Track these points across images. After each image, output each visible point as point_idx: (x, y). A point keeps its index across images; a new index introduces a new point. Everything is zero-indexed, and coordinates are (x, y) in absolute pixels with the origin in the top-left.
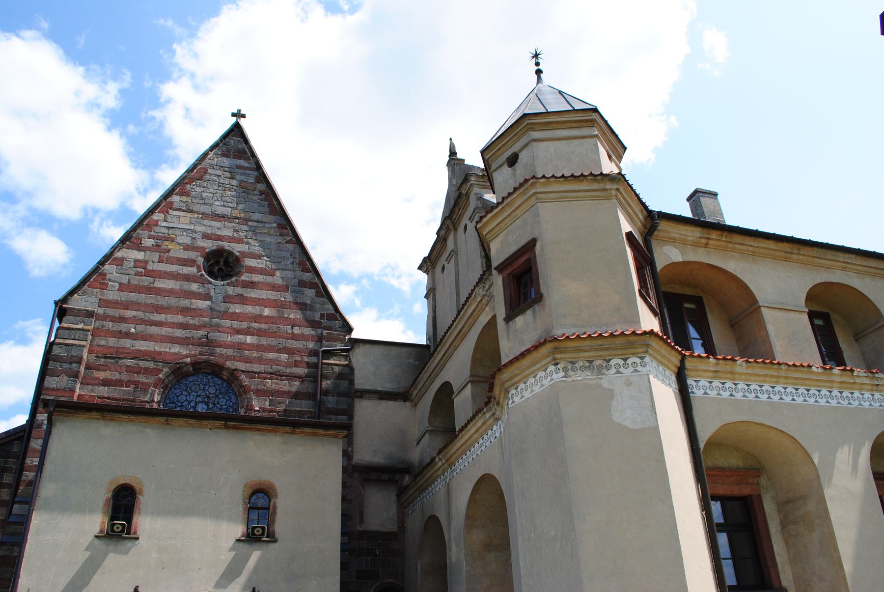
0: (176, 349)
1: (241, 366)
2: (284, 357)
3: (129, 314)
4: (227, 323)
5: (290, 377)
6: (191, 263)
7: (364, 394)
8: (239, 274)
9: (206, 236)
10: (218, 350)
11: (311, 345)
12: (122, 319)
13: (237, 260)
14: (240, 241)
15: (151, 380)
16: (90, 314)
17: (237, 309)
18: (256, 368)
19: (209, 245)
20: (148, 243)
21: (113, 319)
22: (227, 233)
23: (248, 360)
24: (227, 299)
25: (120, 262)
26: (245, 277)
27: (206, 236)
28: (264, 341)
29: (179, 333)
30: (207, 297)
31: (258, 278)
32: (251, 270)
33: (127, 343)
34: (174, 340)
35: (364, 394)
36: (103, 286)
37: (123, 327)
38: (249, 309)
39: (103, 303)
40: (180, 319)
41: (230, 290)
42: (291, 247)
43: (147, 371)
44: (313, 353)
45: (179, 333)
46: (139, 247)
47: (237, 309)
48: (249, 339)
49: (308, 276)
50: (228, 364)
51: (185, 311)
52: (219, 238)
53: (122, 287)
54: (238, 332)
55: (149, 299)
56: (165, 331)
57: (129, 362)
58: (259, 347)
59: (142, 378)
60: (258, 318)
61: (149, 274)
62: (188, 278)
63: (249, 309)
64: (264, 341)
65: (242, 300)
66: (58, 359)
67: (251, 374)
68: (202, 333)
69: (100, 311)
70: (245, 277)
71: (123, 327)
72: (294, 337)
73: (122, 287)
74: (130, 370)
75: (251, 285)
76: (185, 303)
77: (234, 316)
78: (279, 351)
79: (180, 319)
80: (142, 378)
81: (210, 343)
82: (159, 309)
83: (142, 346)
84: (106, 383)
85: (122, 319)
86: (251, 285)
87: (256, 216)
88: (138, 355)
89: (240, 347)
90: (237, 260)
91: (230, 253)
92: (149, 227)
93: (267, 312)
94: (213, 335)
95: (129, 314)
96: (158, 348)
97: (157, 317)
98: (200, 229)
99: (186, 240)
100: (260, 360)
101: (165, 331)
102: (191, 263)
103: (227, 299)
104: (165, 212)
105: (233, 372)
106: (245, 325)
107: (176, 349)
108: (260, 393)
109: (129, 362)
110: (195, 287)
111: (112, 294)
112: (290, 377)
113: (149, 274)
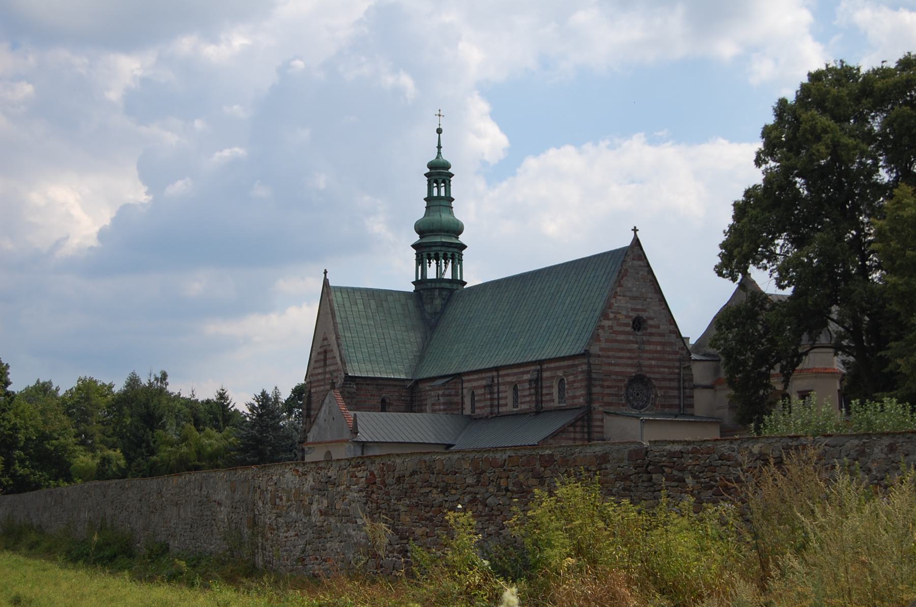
0: (629, 370)
1: (653, 376)
2: (666, 370)
3: (611, 353)
4: (645, 355)
5: (671, 380)
6: (627, 325)
7: (695, 387)
8: (646, 329)
9: (633, 310)
10: (644, 369)
11: (677, 364)
12: (609, 357)
13: (645, 321)
14: (644, 310)
15: (623, 384)
16: (599, 356)
17: (648, 347)
18: (658, 376)
19: (633, 314)
20: (612, 316)
21: (606, 357)
22: (639, 307)
23: (654, 373)
24: (643, 343)
25: (603, 327)
26: (649, 331)
27: (633, 310)
28: (660, 363)
29: (629, 362)
30: (637, 343)
31: (654, 330)
32: (651, 326)
33: (612, 368)
34: (628, 365)
35: (695, 387)
36: (600, 341)
37: (609, 360)
38: (652, 347)
39: (601, 349)
40: (628, 354)
41: (645, 338)
42: (664, 311)
43: (620, 381)
44: (679, 368)
45: (629, 362)
46: (609, 319)
47: (648, 347)
48: (653, 362)
49: (672, 327)
50: (648, 375)
51: (630, 350)
52: (637, 310)
53: (607, 340)
54: (650, 359)
55: (616, 345)
56: (624, 361)
57: (613, 377)
58: (658, 367)
59: (619, 384)
60: (656, 352)
61: (614, 332)
62: (628, 333)
63: (652, 347)
64: (660, 363)
65: (650, 343)
66: (595, 379)
67: (656, 379)
68: (635, 361)
69: (600, 353)
70: (649, 331)
71: (609, 360)
72: (669, 360)
73: (607, 340)
74: (615, 380)
75: (651, 334)
76: (629, 346)
77: (647, 351)
78: (665, 367)
79: (628, 354)
80: (619, 384)
81: (639, 366)
82: (622, 350)
83: (617, 369)
84: (608, 387)
85: (609, 357)
86: (651, 334)
87: (650, 295)
88: (617, 373)
89: (651, 366)
90: (645, 321)
91: (642, 318)
92: (610, 307)
93: (659, 348)
94: (641, 361)
95: (611, 353)
96: (623, 369)
97: (621, 354)
98: (629, 306)
99: (624, 313)
100: (658, 373)
101: (624, 361)
102: (627, 325)
103: (643, 343)
104: (615, 297)
105: (649, 379)
106: (651, 356)
107: (629, 370)
108: (660, 388)
109: (613, 377)
110: (631, 338)
111: (603, 345)
112: (671, 380)
113: (614, 332)
